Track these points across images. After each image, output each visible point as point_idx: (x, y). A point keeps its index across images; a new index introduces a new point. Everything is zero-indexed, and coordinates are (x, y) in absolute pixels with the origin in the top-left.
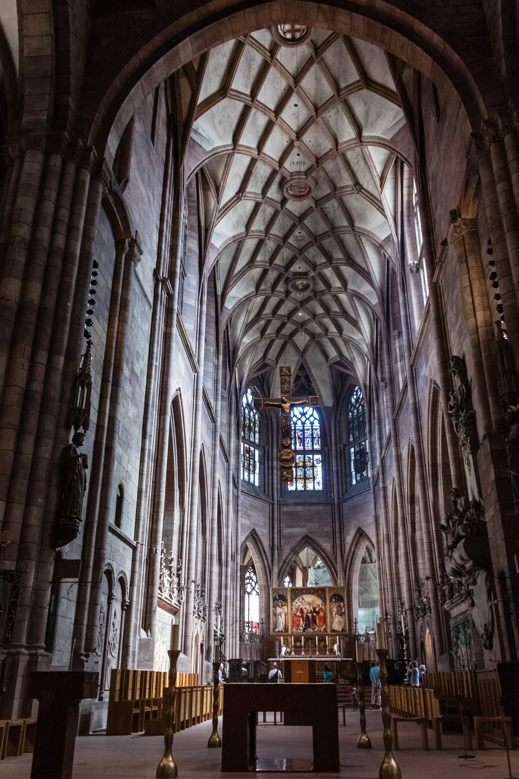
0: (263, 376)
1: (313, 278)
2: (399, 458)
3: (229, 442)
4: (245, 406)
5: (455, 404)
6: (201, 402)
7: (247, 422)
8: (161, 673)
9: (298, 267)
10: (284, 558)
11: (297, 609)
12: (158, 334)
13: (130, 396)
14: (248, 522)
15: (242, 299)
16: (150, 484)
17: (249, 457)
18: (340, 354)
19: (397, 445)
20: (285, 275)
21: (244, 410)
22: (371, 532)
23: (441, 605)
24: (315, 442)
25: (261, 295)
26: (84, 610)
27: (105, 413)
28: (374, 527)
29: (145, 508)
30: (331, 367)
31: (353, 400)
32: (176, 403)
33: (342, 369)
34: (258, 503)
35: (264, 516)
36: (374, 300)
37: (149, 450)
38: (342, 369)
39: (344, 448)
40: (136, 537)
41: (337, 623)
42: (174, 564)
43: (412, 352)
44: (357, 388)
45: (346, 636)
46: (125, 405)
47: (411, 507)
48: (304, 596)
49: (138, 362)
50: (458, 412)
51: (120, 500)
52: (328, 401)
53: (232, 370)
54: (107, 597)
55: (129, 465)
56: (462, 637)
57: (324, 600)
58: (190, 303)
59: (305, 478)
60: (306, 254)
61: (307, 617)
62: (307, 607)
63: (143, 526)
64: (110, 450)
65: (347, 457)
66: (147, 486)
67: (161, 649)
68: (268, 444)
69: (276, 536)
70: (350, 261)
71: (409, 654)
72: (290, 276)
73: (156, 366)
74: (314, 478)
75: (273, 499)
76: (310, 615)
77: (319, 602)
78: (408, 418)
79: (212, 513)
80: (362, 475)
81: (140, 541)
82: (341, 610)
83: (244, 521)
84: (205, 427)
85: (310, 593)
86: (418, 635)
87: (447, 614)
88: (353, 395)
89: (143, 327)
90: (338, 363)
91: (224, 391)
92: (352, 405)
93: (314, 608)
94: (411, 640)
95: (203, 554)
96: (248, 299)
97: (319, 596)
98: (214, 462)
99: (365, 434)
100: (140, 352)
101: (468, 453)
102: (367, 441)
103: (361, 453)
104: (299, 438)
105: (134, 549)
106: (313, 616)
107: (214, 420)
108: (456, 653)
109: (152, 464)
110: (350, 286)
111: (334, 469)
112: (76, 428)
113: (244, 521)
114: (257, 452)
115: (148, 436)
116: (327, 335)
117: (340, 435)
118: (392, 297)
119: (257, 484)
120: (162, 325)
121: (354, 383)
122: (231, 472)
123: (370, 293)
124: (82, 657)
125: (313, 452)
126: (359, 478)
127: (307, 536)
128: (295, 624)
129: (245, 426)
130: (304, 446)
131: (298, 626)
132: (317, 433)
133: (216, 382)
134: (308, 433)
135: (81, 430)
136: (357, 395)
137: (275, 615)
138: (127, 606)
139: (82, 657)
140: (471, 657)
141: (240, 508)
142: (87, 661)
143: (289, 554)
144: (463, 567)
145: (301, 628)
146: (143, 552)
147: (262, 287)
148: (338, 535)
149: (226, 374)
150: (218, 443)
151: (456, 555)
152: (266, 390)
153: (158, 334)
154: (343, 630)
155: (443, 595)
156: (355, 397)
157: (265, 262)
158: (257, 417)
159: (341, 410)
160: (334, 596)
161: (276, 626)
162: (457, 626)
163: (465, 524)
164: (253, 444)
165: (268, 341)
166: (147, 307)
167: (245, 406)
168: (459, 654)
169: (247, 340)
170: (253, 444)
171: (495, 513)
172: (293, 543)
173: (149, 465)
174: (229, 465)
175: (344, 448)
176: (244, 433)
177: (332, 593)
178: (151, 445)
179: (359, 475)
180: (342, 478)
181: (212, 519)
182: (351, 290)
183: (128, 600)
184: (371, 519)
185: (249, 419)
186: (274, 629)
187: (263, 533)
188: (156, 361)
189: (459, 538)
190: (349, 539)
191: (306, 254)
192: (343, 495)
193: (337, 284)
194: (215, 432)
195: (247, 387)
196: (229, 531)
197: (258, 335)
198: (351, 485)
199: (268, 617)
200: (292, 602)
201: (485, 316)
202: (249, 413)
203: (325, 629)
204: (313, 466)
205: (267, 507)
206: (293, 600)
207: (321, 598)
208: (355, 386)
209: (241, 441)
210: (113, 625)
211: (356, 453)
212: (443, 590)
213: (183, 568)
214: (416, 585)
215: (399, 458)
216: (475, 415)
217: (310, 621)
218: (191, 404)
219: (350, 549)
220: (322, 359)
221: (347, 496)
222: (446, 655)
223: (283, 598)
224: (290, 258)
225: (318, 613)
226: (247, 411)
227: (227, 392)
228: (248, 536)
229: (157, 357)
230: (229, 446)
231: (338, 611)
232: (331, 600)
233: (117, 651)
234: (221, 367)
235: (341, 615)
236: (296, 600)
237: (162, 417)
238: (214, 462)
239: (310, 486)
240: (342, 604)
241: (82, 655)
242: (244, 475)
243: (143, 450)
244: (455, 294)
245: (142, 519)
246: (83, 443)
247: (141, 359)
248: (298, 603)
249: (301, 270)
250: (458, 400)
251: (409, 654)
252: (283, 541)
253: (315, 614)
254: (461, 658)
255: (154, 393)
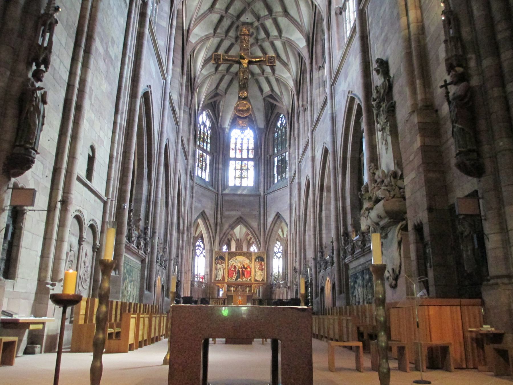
0: (215, 102)
1: (257, 28)
2: (313, 159)
3: (188, 145)
4: (201, 123)
5: (377, 97)
6: (167, 103)
7: (202, 135)
8: (125, 303)
9: (247, 18)
10: (224, 231)
11: (232, 266)
12: (133, 31)
13: (104, 73)
14: (200, 205)
15: (203, 37)
16: (121, 152)
17: (202, 160)
18: (272, 90)
19: (313, 149)
20: (236, 23)
21: (200, 126)
22: (286, 216)
23: (343, 260)
24: (250, 152)
25: (218, 37)
26: (50, 245)
27: (75, 74)
28: (288, 212)
29: (115, 171)
30: (264, 99)
31: (279, 125)
32: (146, 96)
33: (272, 101)
34: (207, 193)
35: (212, 202)
36: (302, 43)
37: (121, 124)
38: (272, 101)
39: (270, 158)
40: (107, 194)
41: (259, 275)
42: (141, 223)
43: (332, 76)
44: (282, 115)
45: (264, 284)
46: (99, 78)
47: (320, 194)
48: (237, 257)
49: (113, 46)
50: (380, 102)
51: (91, 160)
52: (261, 124)
53: (193, 93)
54: (78, 239)
55: (101, 132)
56: (360, 281)
57: (251, 260)
58: (163, 25)
59: (241, 177)
60: (253, 7)
61: (239, 271)
62: (239, 264)
63: (114, 185)
64: (79, 108)
65: (272, 164)
66: (117, 153)
67: (129, 286)
68: (216, 152)
69: (219, 216)
70: (286, 13)
71: (312, 296)
72: (240, 24)
73: (129, 56)
74: (247, 178)
75: (218, 191)
76: (240, 270)
77: (247, 261)
78: (325, 125)
79: (173, 193)
80: (282, 176)
81: (110, 197)
82: (262, 267)
83: (197, 204)
84: (170, 125)
85: (241, 255)
86: (319, 282)
87: (347, 266)
88: (278, 120)
89: (119, 18)
90: (271, 96)
91: (186, 107)
92: (278, 127)
93: (243, 266)
94: (313, 286)
95: (165, 222)
96: (207, 38)
97: (247, 257)
98: (176, 155)
99: (286, 148)
100: (115, 39)
101: (387, 135)
102: (287, 153)
103: (283, 161)
104: (239, 149)
105: (105, 203)
106: (242, 271)
107: (177, 124)
108: (353, 293)
109: (122, 137)
110: (284, 35)
111: (262, 171)
112: (38, 66)
113: (197, 204)
114: (208, 158)
115: (120, 112)
116: (263, 74)
117: (268, 149)
118: (316, 41)
119: (207, 179)
120: (136, 24)
121: (280, 112)
122: (189, 167)
123: (299, 39)
124: (47, 286)
125: (248, 159)
126: (279, 179)
127: (241, 217)
128: (230, 275)
129: (200, 138)
130: (242, 155)
131: (232, 277)
132: (252, 146)
133: (180, 95)
134: (245, 147)
135: (42, 67)
136: (281, 120)
137: (216, 269)
138: (98, 249)
139: (49, 286)
140: (366, 295)
141: (194, 195)
142: (53, 289)
143: (228, 229)
144: (377, 224)
145: (234, 279)
146: (113, 207)
147: (218, 31)
148: (262, 217)
149: (188, 95)
150: (180, 141)
151: (373, 214)
152: (217, 113)
153: (133, 31)
154: (263, 280)
155: (345, 252)
156: (280, 122)
157: (222, 10)
158: (209, 132)
159: (269, 131)
160: (258, 257)
161: (216, 277)
162: (356, 274)
163: (384, 189)
164: (205, 151)
165: (221, 76)
166: (123, 5)
167: (201, 123)
168: (356, 293)
169: (205, 72)
170: (205, 151)
171: (417, 175)
172: (231, 221)
173: (120, 136)
174: (187, 162)
175: (270, 158)
176: (200, 142)
177: (257, 256)
178: (122, 120)
179: (279, 176)
180: (267, 179)
181: (174, 197)
182: (285, 37)
183: (98, 244)
184: (287, 207)
185: (204, 133)
186: (215, 278)
187: (210, 212)
188: (130, 52)
189: (377, 201)
190: (270, 220)
191: (253, 7)
192: (267, 189)
193: (274, 32)
194: (178, 132)
195: (203, 109)
196: (186, 209)
197: (213, 70)
198: (274, 183)
199: (211, 270)
200: (228, 261)
201: (416, 14)
202: (204, 129)
203: (250, 279)
204: (247, 169)
205: (214, 196)
206: (229, 260)
207: (249, 259)
208: (281, 114)
209: (197, 147)
210: (84, 262)
211: (278, 161)
212: (345, 249)
213: (149, 228)
214: (320, 249)
215: (313, 159)
216: (395, 104)
217: (240, 274)
218: (160, 103)
219: (271, 226)
220: (259, 93)
221: (271, 190)
222: (343, 295)
223: (222, 258)
224: (241, 9)
225: (246, 269)
226: (202, 127)
227: (188, 108)
228: (199, 215)
229: (130, 49)
230: (188, 148)
231: (260, 267)
232: (255, 261)
233: (88, 284)
234: (184, 85)
235: (262, 270)
236: (231, 260)
237: (133, 100)
238: (176, 155)
239: (244, 184)
240: (263, 263)
241: (48, 284)
242: (198, 172)
243: (115, 123)
244: (383, 9)
245: (112, 179)
246: (43, 79)
247: (115, 45)
248: (232, 262)
249: (249, 21)
250: (380, 94)
251: (312, 296)
252: (223, 220)
253: (244, 269)
254: (357, 296)
255: (126, 78)
